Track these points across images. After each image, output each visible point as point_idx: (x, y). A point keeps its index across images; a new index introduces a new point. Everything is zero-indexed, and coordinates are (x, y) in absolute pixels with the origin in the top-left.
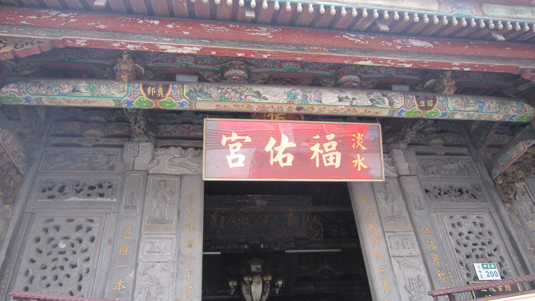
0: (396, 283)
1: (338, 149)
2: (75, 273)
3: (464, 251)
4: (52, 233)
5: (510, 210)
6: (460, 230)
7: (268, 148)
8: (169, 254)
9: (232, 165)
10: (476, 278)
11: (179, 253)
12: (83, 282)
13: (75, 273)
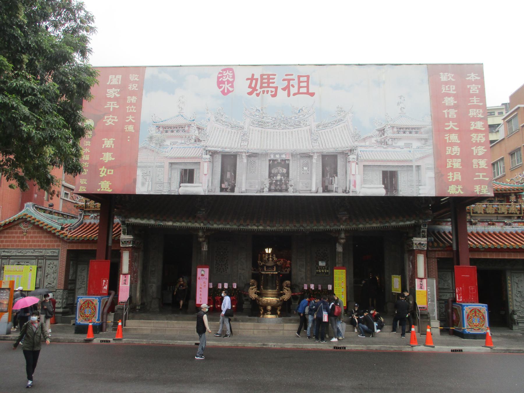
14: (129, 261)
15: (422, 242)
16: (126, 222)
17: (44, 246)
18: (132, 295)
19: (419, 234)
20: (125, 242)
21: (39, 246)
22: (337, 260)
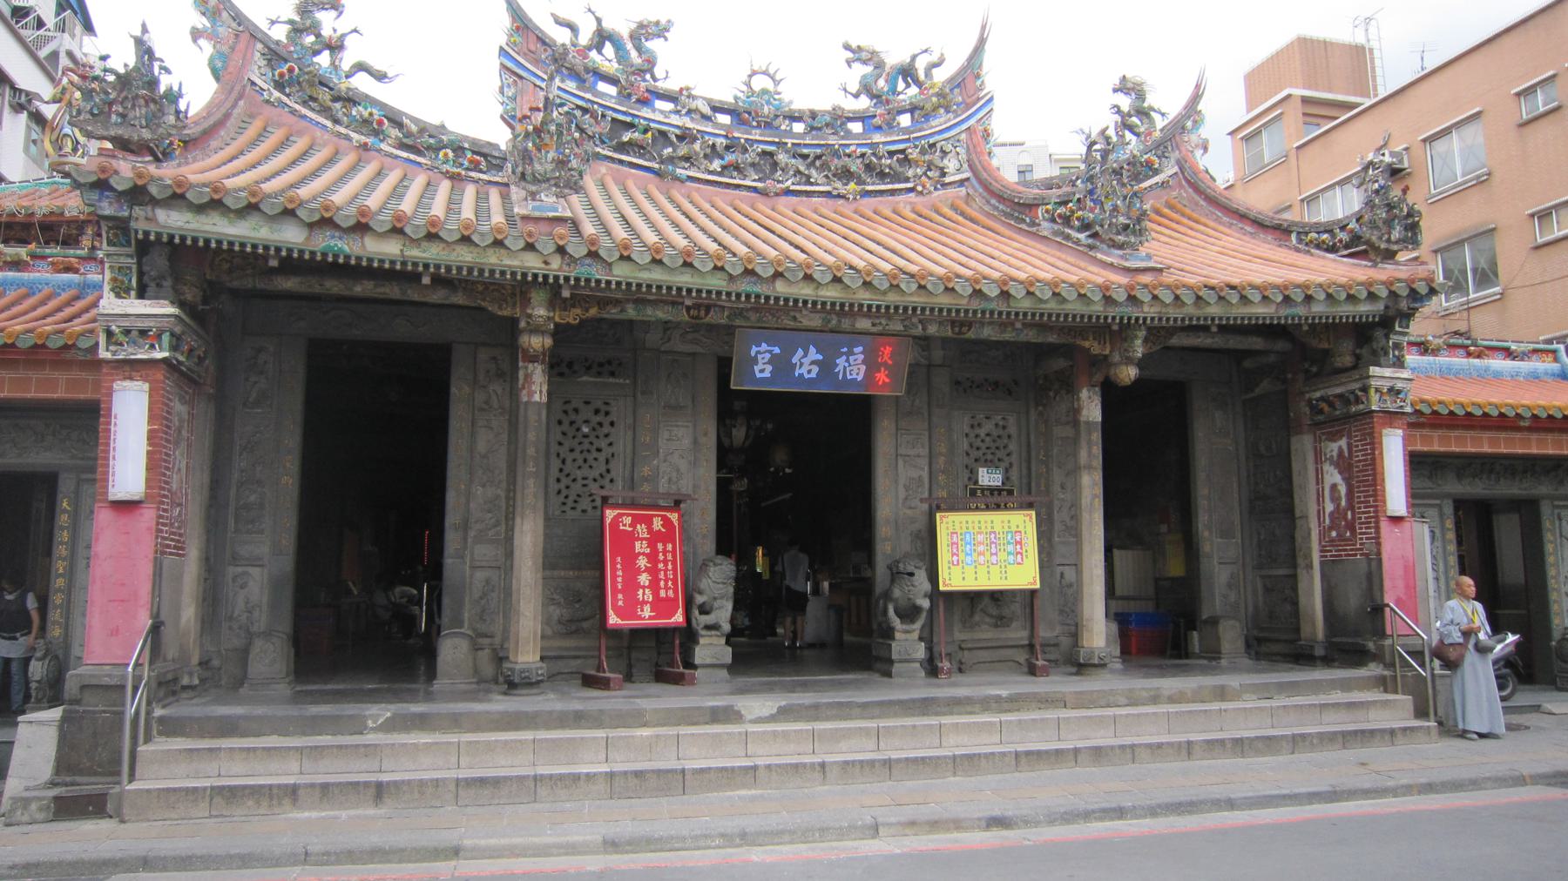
0: (896, 482)
1: (864, 362)
2: (602, 457)
3: (975, 454)
4: (573, 417)
5: (1041, 414)
6: (977, 431)
7: (795, 360)
8: (687, 442)
9: (759, 375)
10: (976, 482)
11: (695, 442)
12: (611, 466)
13: (602, 457)
14: (152, 437)
18: (163, 617)
20: (127, 332)
22: (1083, 455)
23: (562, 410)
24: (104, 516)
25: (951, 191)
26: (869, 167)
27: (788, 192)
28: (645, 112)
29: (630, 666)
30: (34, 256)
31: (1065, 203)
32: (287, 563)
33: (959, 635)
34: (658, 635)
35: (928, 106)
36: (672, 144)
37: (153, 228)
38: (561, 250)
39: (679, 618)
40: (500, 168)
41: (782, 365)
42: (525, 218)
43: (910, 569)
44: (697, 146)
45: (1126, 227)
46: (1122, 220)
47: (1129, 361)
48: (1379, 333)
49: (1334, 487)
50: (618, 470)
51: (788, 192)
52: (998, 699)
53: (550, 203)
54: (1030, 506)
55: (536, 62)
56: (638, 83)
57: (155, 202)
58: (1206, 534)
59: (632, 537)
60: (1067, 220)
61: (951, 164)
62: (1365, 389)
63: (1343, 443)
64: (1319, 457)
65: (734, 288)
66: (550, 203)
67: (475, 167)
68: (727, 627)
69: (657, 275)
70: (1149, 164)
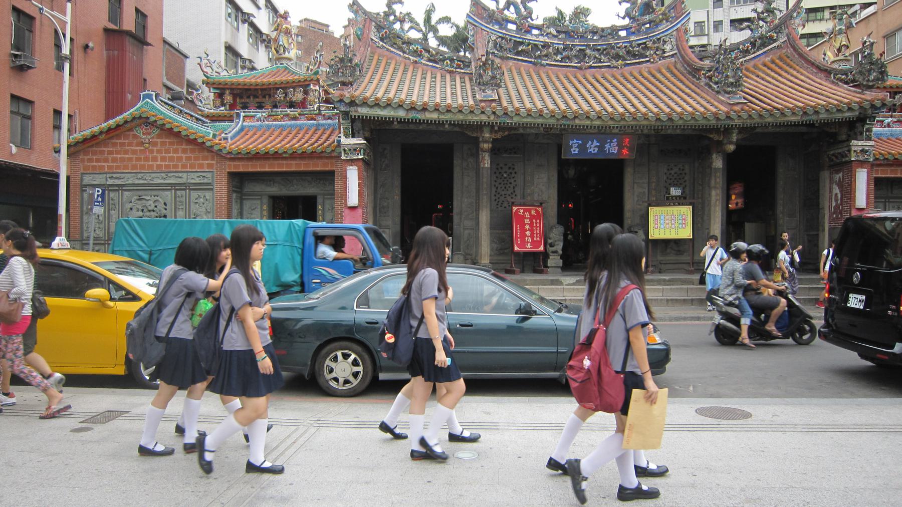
8: (545, 180)
11: (549, 179)
12: (516, 189)
15: (867, 149)
16: (353, 114)
17: (184, 166)
19: (861, 134)
21: (176, 166)
22: (713, 182)
23: (496, 168)
24: (346, 212)
25: (667, 60)
26: (628, 52)
27: (591, 67)
28: (529, 37)
29: (523, 267)
30: (300, 114)
31: (710, 71)
32: (398, 228)
33: (660, 258)
34: (534, 255)
35: (658, 20)
36: (539, 50)
37: (357, 114)
38: (494, 113)
39: (542, 248)
40: (469, 66)
41: (582, 148)
42: (481, 101)
43: (636, 230)
44: (550, 50)
45: (732, 83)
46: (731, 80)
47: (731, 143)
48: (858, 125)
49: (836, 194)
50: (518, 191)
51: (591, 67)
52: (664, 280)
53: (492, 94)
54: (690, 204)
55: (481, 19)
56: (524, 24)
57: (357, 105)
58: (781, 216)
59: (523, 217)
60: (710, 78)
61: (668, 47)
62: (849, 151)
63: (841, 175)
64: (831, 182)
65: (559, 123)
66: (492, 94)
67: (459, 67)
68: (560, 252)
69: (529, 120)
70: (771, 37)
